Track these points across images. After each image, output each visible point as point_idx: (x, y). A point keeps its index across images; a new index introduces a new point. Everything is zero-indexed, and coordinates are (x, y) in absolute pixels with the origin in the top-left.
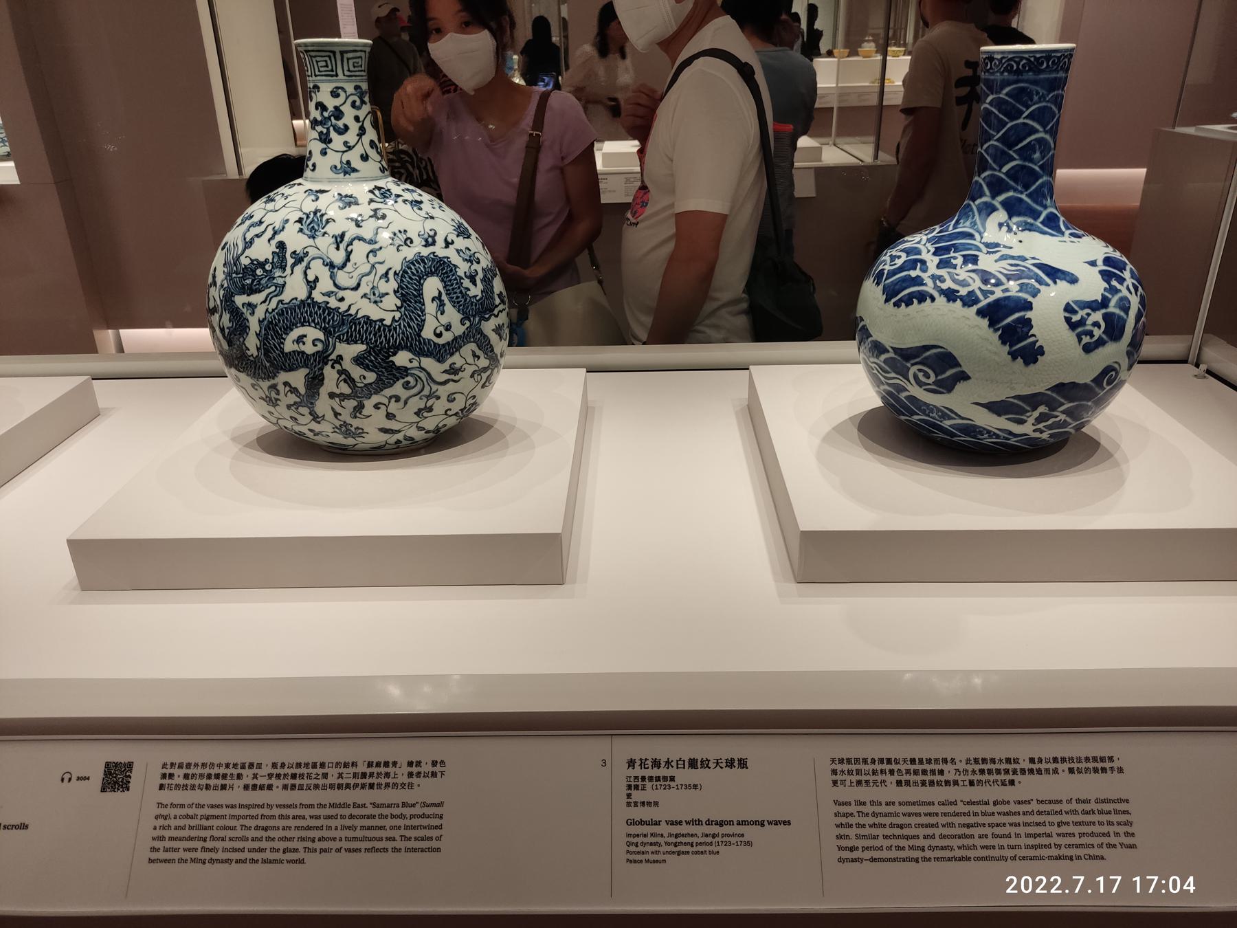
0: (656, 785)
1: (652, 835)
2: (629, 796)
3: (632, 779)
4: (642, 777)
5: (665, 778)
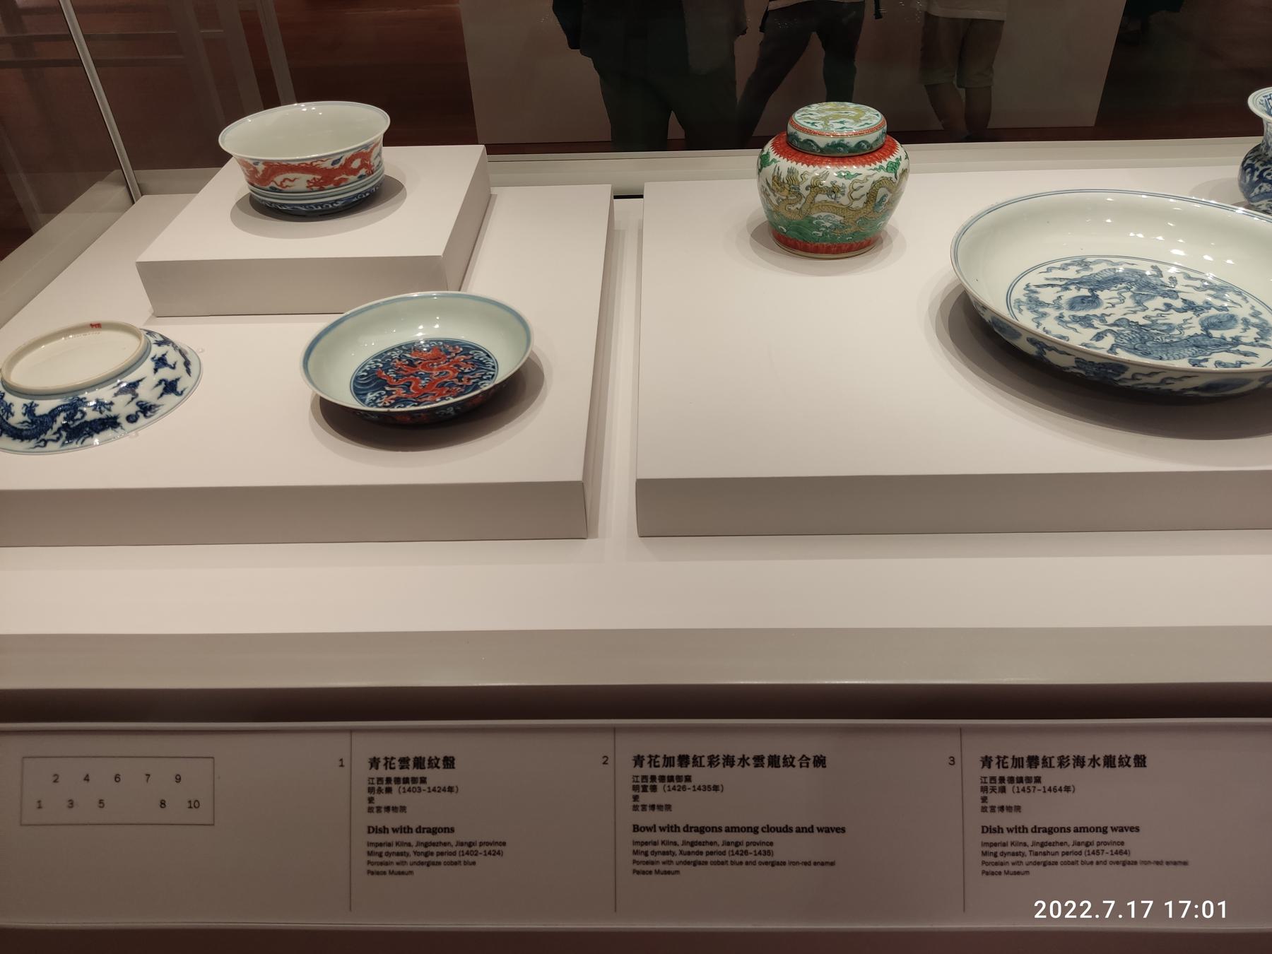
0: (669, 786)
2: (636, 798)
3: (640, 779)
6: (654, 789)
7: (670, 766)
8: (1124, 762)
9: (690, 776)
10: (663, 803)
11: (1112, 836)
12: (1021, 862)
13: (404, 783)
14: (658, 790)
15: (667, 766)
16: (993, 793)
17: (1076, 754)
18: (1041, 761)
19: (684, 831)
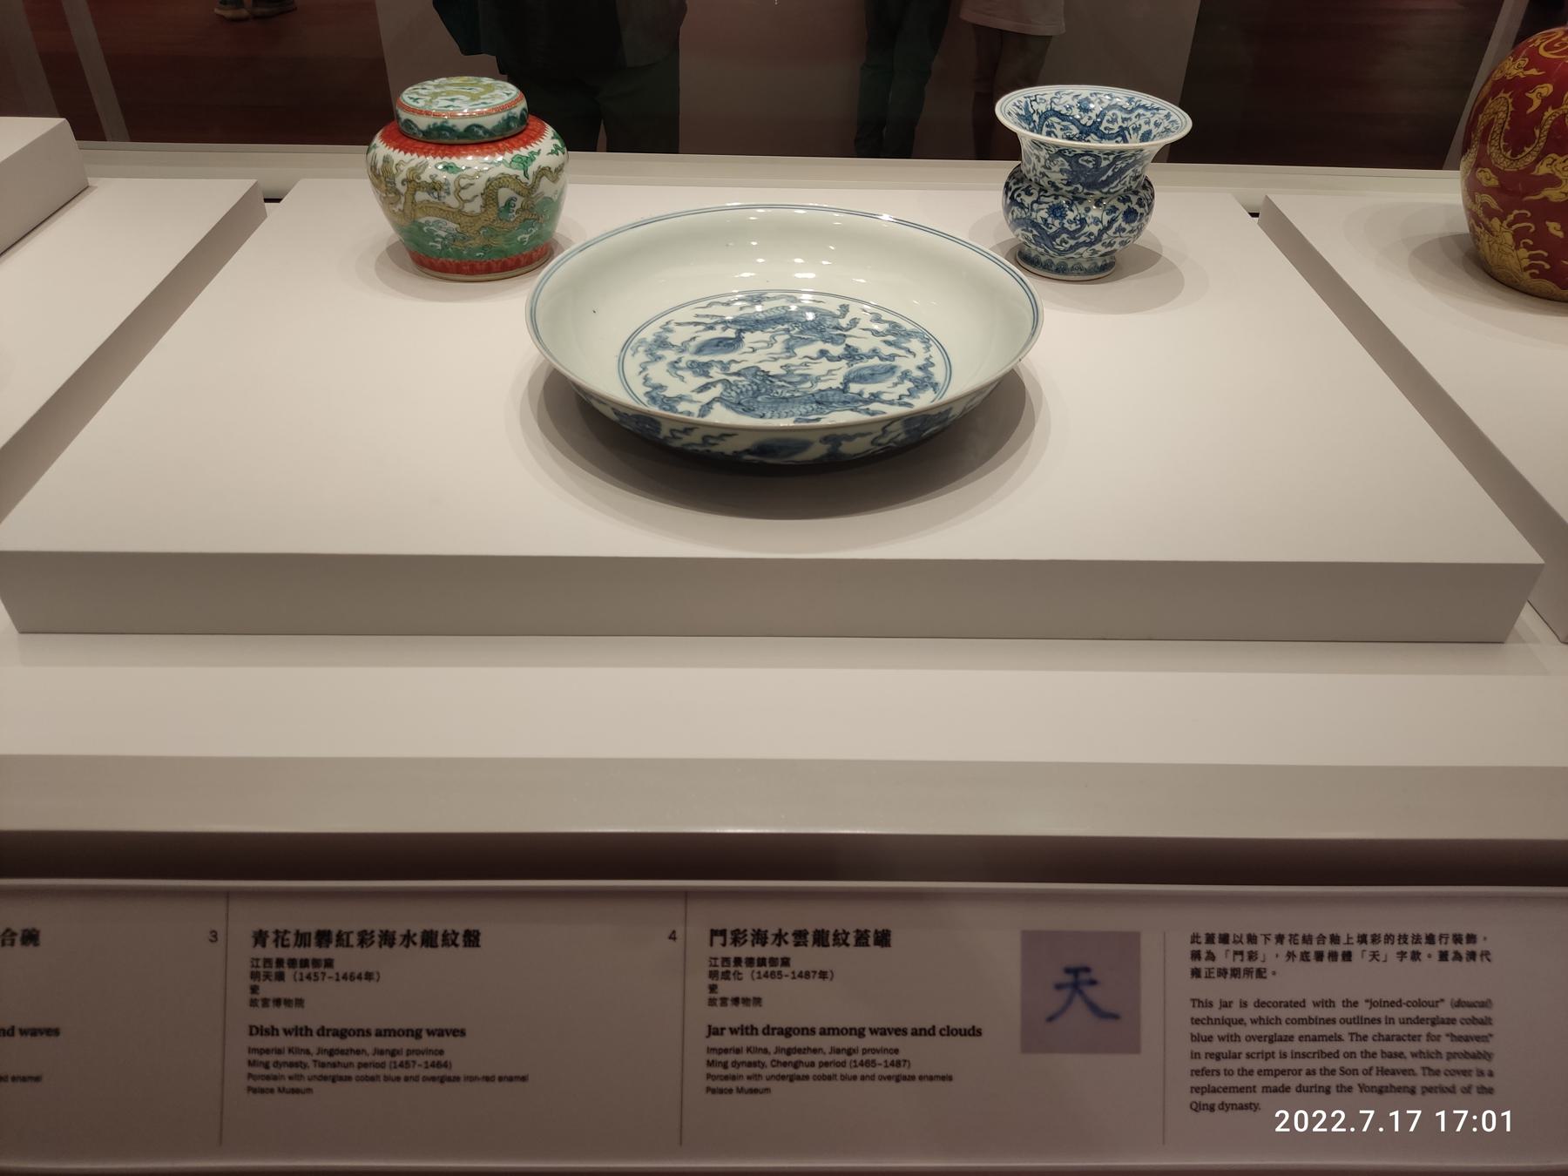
2: (713, 988)
5: (773, 961)
7: (305, 946)
8: (449, 939)
10: (751, 995)
11: (427, 1042)
12: (302, 1076)
13: (301, 967)
15: (299, 946)
16: (268, 981)
17: (384, 929)
18: (334, 938)
19: (764, 1034)
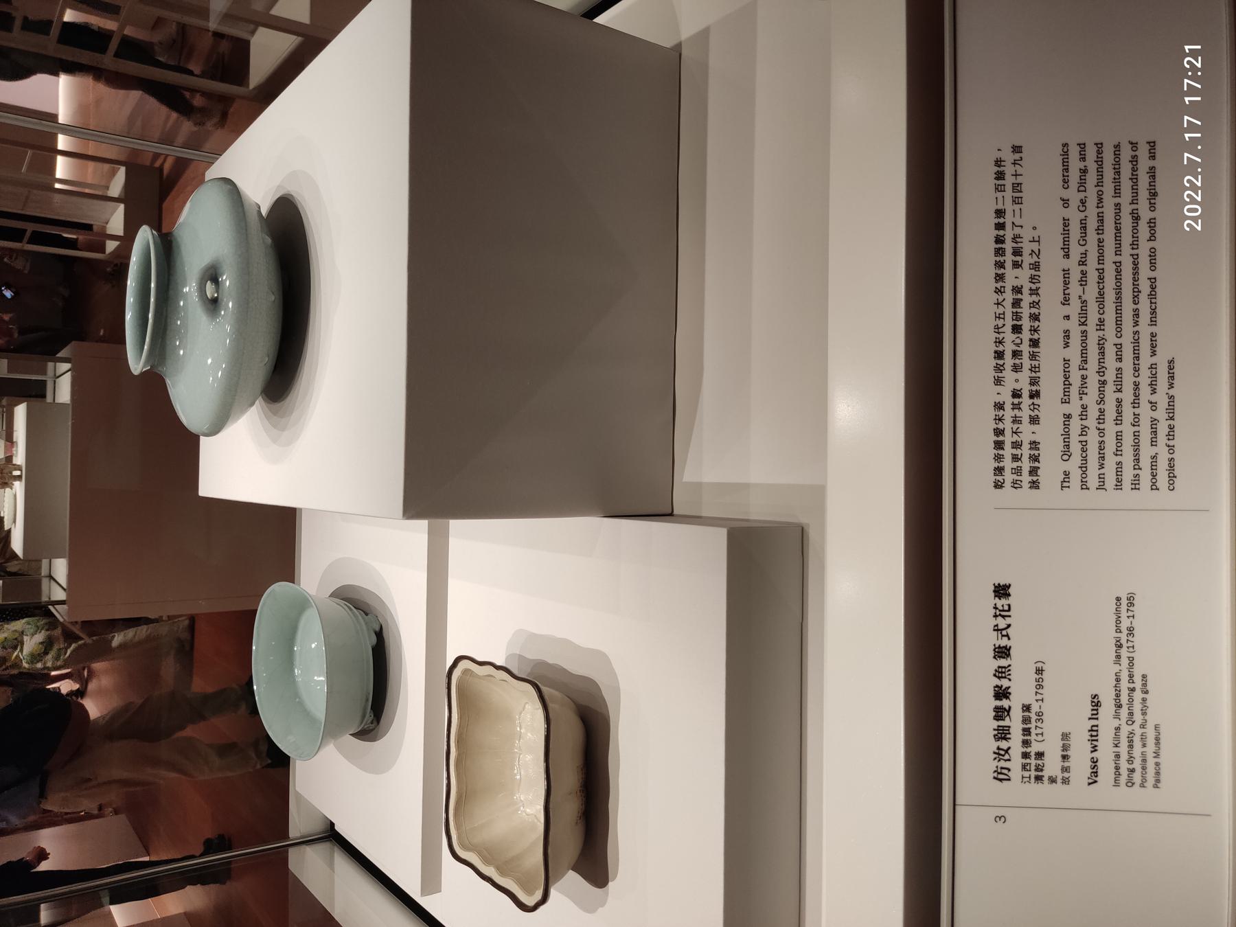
0: (1037, 734)
1: (1116, 746)
2: (1053, 780)
4: (1023, 758)
5: (1026, 720)
6: (1040, 755)
9: (1024, 706)
14: (1041, 750)
